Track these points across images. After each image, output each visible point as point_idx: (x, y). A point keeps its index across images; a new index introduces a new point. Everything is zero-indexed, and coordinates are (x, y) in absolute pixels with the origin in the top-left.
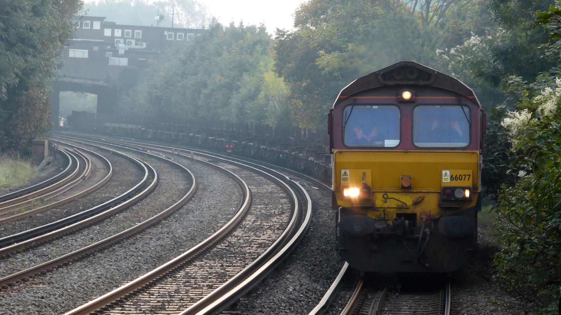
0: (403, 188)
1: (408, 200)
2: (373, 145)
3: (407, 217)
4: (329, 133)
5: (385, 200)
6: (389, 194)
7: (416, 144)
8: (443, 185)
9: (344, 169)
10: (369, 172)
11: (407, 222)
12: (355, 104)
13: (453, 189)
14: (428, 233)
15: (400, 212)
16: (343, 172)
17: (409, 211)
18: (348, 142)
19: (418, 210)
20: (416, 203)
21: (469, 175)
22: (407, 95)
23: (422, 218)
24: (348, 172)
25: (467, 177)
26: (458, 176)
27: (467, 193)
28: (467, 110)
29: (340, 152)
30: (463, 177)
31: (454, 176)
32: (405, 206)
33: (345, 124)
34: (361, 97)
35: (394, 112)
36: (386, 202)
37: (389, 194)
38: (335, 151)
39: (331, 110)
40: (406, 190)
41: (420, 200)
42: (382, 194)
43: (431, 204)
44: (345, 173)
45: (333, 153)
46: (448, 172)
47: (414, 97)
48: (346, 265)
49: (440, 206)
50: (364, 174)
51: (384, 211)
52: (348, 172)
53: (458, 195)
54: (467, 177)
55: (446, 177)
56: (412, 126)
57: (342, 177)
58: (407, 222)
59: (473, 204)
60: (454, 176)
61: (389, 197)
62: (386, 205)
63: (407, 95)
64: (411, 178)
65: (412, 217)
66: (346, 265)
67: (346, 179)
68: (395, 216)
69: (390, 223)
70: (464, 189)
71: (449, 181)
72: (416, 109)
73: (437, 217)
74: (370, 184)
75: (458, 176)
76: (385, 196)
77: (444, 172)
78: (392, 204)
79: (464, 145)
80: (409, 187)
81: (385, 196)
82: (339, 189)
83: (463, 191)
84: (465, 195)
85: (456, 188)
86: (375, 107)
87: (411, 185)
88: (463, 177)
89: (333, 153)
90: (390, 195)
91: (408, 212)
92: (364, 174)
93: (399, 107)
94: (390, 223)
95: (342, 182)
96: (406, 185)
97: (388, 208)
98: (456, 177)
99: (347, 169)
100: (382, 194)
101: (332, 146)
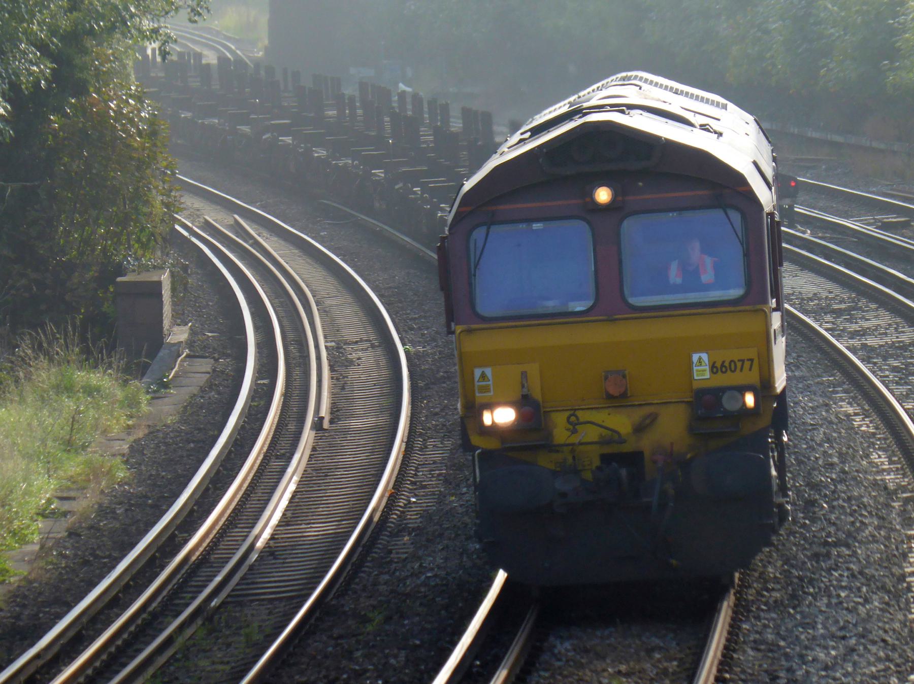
0: (610, 397)
1: (621, 422)
2: (540, 311)
3: (622, 461)
4: (442, 289)
5: (574, 426)
6: (579, 414)
7: (633, 301)
8: (695, 386)
9: (480, 366)
10: (533, 370)
11: (624, 472)
12: (492, 221)
13: (718, 392)
14: (671, 492)
15: (607, 450)
16: (478, 373)
17: (627, 448)
18: (487, 306)
19: (646, 444)
20: (640, 429)
21: (752, 360)
22: (603, 195)
23: (655, 462)
24: (488, 372)
25: (747, 364)
26: (727, 364)
27: (750, 400)
28: (736, 217)
29: (469, 331)
30: (739, 365)
31: (718, 365)
32: (616, 437)
33: (476, 267)
34: (501, 207)
35: (577, 233)
36: (574, 431)
37: (579, 414)
38: (459, 329)
39: (443, 239)
40: (618, 400)
41: (648, 421)
42: (567, 414)
43: (672, 428)
44: (483, 376)
45: (453, 333)
46: (705, 356)
47: (620, 198)
48: (501, 576)
49: (691, 430)
50: (524, 374)
51: (573, 451)
52: (488, 372)
53: (728, 404)
54: (747, 364)
55: (701, 368)
56: (620, 262)
57: (477, 384)
58: (624, 472)
59: (765, 420)
60: (718, 365)
61: (581, 420)
62: (574, 439)
63: (603, 195)
64: (624, 376)
65: (634, 459)
66: (501, 576)
67: (486, 389)
68: (597, 462)
69: (588, 476)
70: (742, 390)
71: (707, 375)
72: (626, 224)
73: (689, 456)
74: (537, 395)
75: (727, 364)
76: (573, 419)
77: (695, 357)
78: (591, 434)
79: (735, 292)
80: (624, 395)
81: (573, 419)
82: (474, 410)
83: (736, 394)
84: (744, 403)
85: (722, 390)
86: (537, 226)
87: (626, 390)
88: (739, 365)
89: (453, 333)
90: (583, 416)
91: (625, 451)
92: (524, 374)
93: (588, 223)
94: (588, 476)
95: (477, 394)
96: (614, 391)
97: (581, 444)
98: (722, 365)
99: (486, 366)
100: (567, 414)
101: (451, 316)
